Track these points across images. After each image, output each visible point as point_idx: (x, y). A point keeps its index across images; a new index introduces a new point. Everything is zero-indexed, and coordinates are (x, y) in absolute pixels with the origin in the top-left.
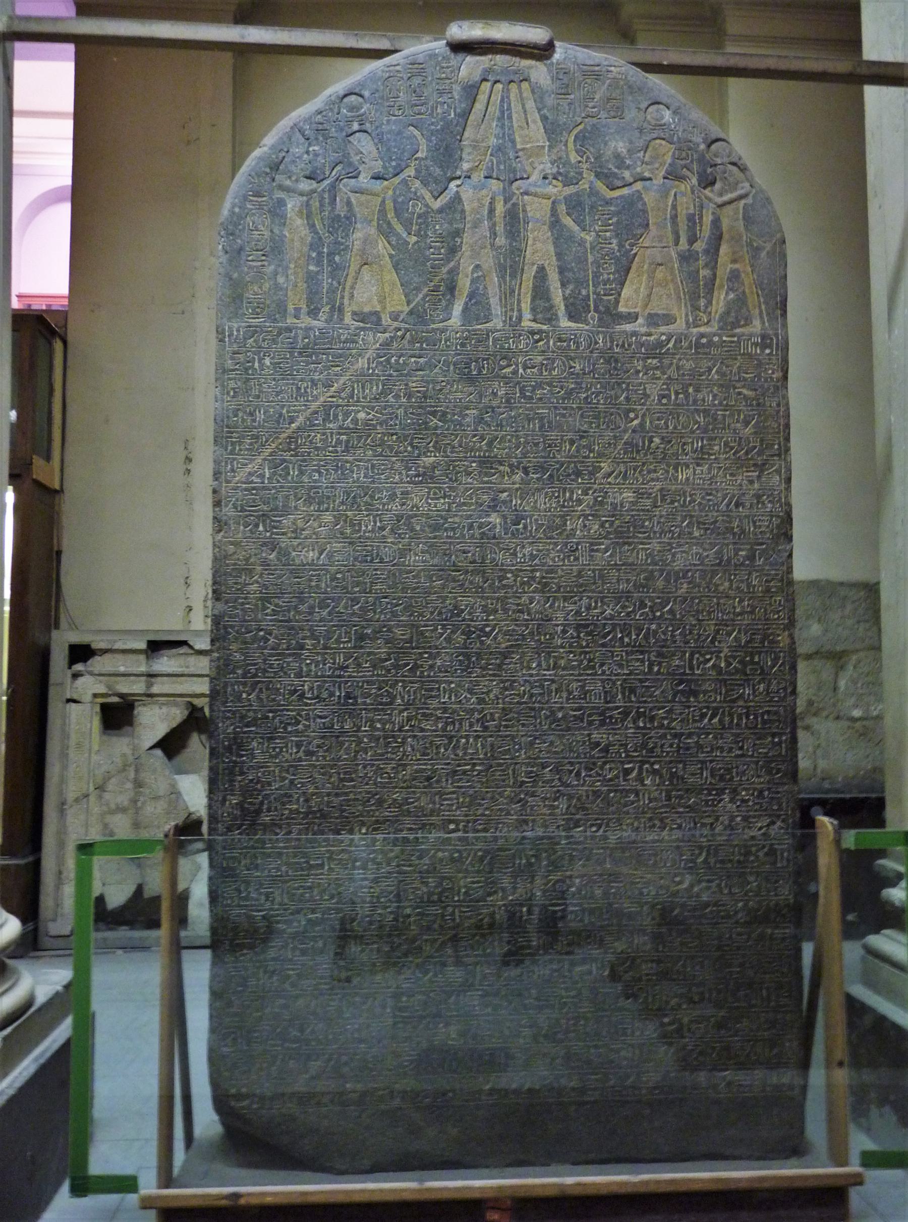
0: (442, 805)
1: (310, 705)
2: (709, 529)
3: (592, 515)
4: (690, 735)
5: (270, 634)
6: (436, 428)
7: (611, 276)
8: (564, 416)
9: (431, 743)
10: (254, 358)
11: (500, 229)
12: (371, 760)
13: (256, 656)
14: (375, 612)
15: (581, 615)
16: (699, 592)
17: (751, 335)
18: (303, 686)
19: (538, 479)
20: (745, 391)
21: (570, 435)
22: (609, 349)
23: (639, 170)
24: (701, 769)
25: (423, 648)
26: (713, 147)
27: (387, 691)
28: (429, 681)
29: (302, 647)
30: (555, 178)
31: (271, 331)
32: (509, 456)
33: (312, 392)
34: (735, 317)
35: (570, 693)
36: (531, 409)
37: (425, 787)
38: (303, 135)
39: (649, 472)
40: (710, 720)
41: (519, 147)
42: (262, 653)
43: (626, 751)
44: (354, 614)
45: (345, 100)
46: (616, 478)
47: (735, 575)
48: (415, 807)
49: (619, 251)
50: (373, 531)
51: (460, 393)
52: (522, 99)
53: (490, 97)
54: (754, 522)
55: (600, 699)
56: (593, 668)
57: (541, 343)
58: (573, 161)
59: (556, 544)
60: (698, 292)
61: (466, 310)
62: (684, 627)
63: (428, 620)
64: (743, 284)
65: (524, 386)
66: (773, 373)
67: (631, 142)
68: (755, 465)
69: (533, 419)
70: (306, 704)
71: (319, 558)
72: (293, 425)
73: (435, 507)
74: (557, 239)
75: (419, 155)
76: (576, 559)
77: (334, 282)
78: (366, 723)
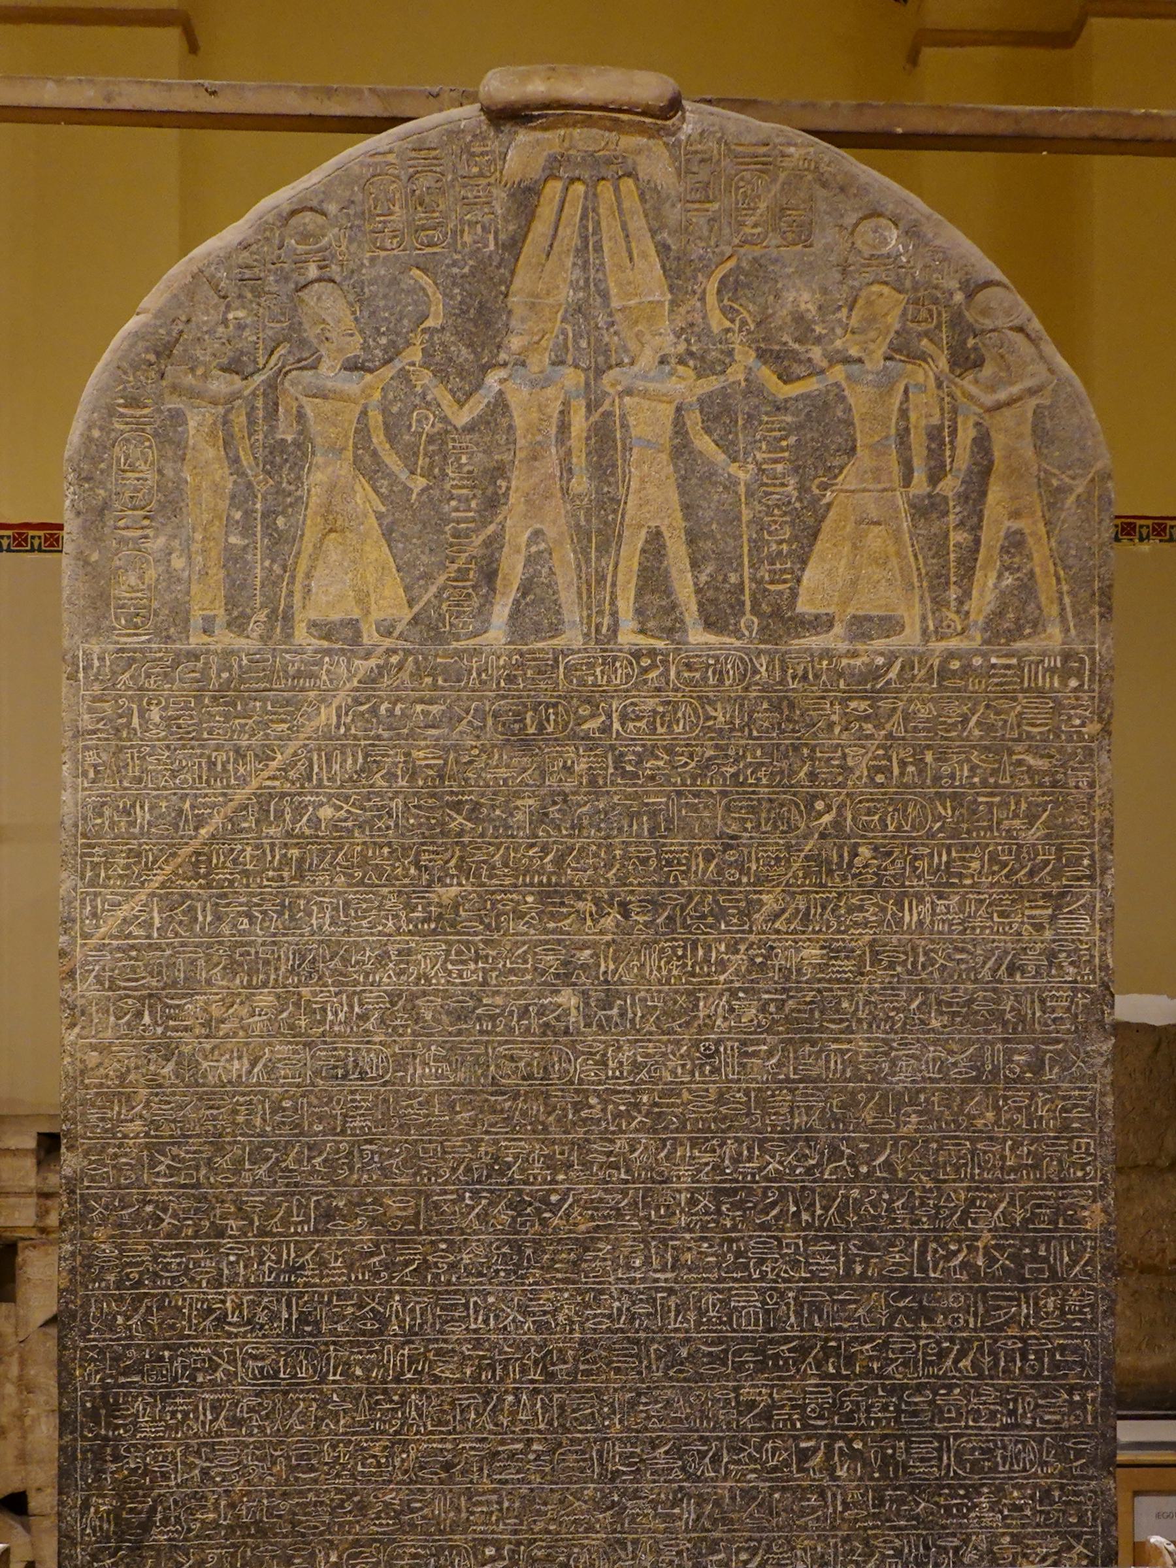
0: (472, 1513)
1: (236, 1336)
2: (958, 1014)
3: (745, 991)
4: (919, 1389)
5: (165, 1210)
6: (461, 834)
7: (785, 547)
8: (694, 808)
9: (452, 1403)
10: (130, 709)
11: (579, 461)
12: (346, 1434)
13: (140, 1249)
14: (351, 1169)
15: (723, 1173)
16: (940, 1129)
17: (1044, 654)
18: (223, 1302)
19: (646, 924)
20: (1031, 760)
21: (706, 844)
22: (780, 683)
23: (838, 343)
24: (939, 1450)
25: (438, 1232)
26: (980, 297)
27: (372, 1310)
28: (448, 1292)
29: (221, 1234)
30: (682, 362)
31: (161, 659)
32: (593, 883)
33: (236, 770)
34: (1014, 619)
35: (702, 1313)
36: (636, 796)
37: (441, 1482)
38: (217, 291)
39: (850, 911)
40: (956, 1362)
41: (615, 304)
42: (151, 1244)
43: (804, 1418)
44: (313, 1172)
45: (293, 222)
46: (789, 921)
47: (1006, 1098)
48: (424, 1517)
49: (799, 499)
50: (346, 1022)
51: (506, 768)
52: (621, 212)
53: (561, 210)
54: (1043, 1001)
55: (757, 1324)
56: (746, 1267)
57: (653, 675)
58: (716, 329)
59: (678, 1043)
60: (946, 576)
61: (516, 613)
62: (912, 1193)
63: (446, 1183)
64: (1030, 557)
65: (622, 755)
66: (1083, 725)
67: (825, 291)
68: (1047, 896)
69: (639, 814)
70: (230, 1335)
71: (250, 1072)
72: (203, 831)
73: (461, 977)
74: (684, 478)
75: (430, 323)
76: (715, 1070)
77: (275, 567)
78: (336, 1368)
